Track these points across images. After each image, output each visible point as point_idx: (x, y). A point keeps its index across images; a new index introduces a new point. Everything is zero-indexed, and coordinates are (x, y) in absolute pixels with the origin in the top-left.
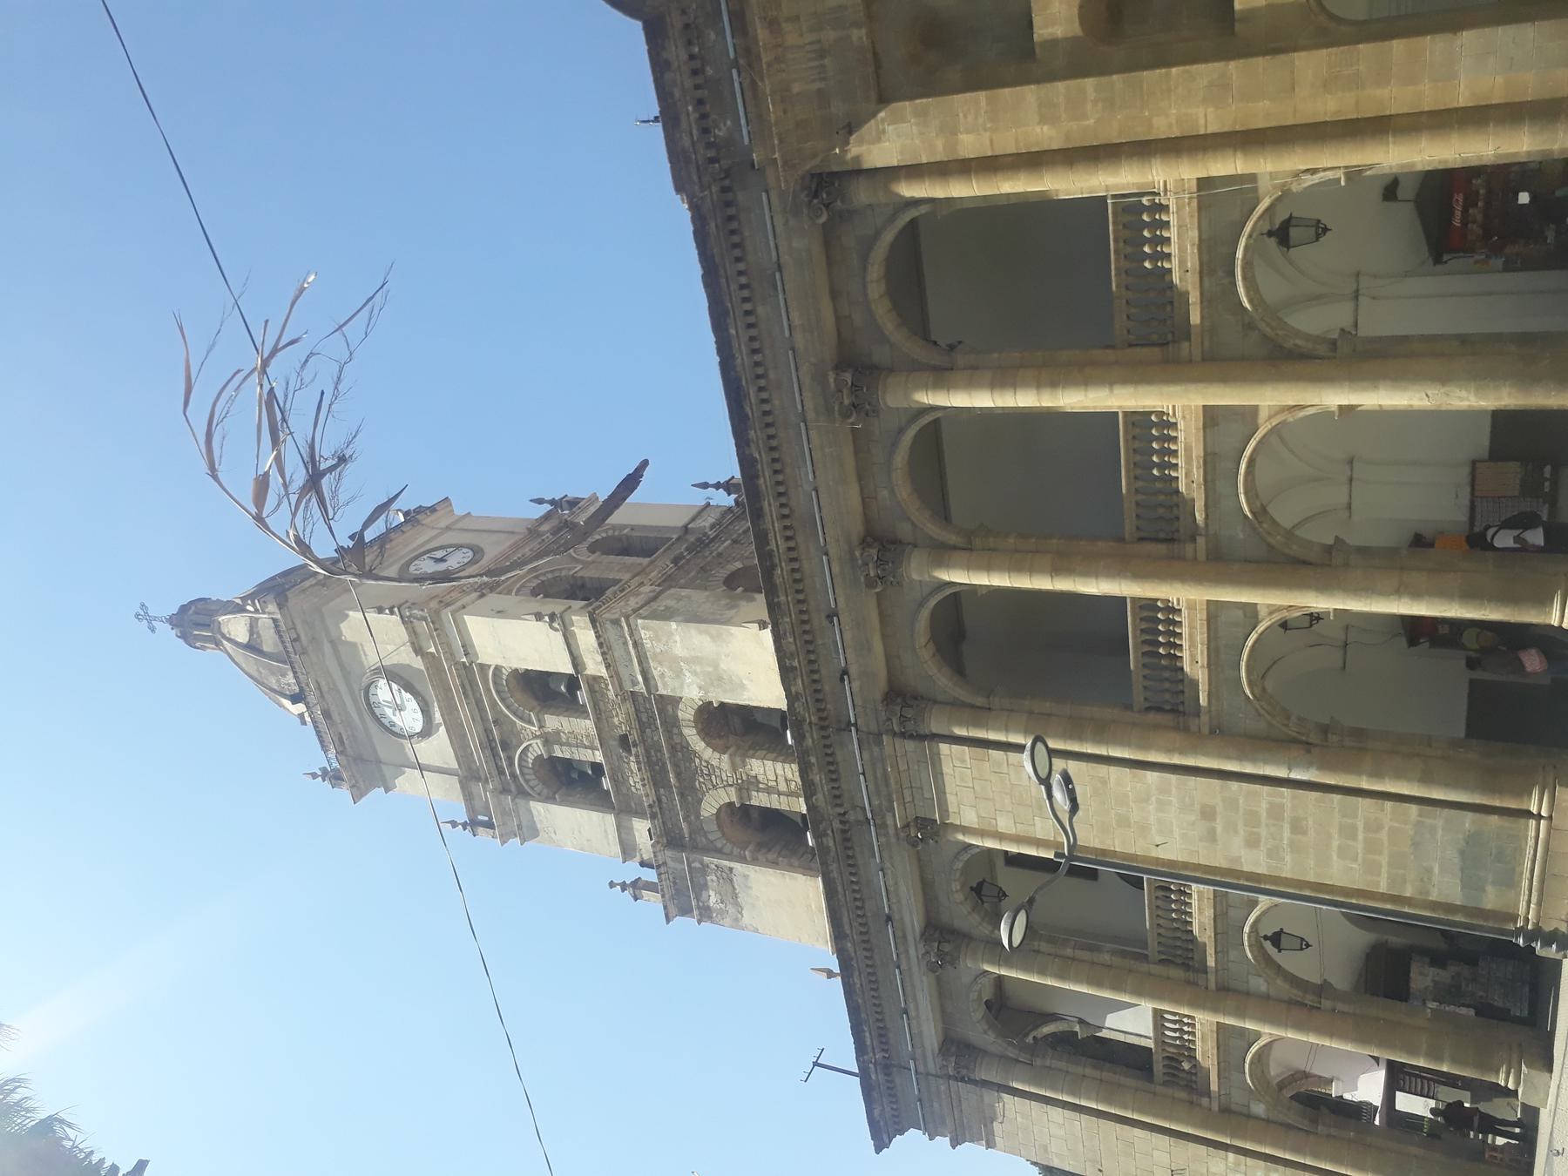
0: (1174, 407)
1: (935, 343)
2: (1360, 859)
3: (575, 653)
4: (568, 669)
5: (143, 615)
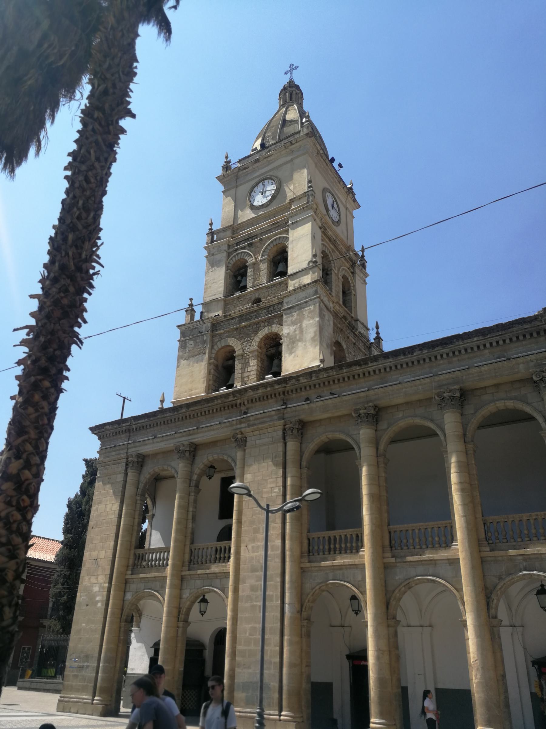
0: (457, 545)
3: (298, 275)
4: (290, 271)
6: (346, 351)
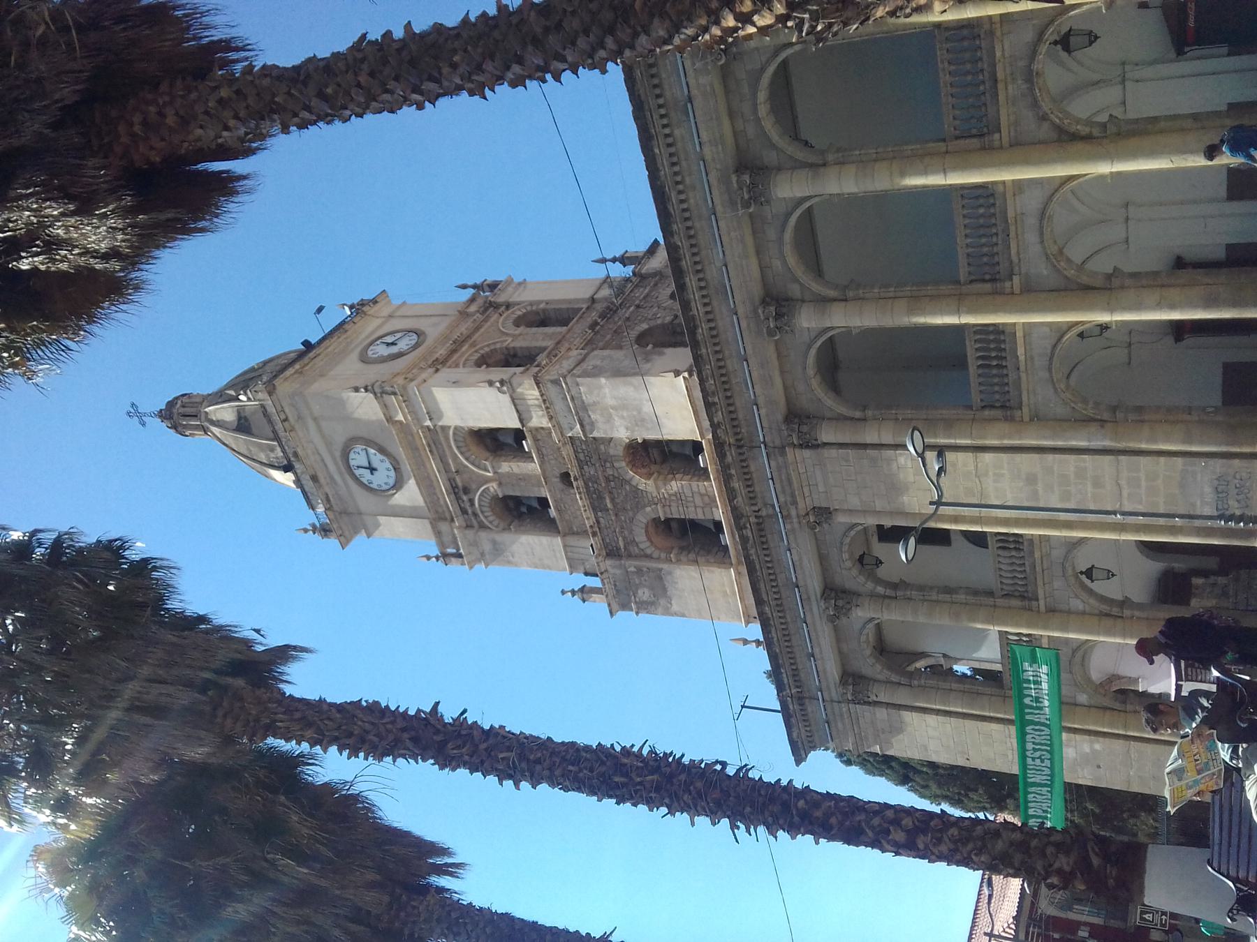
1: (806, 143)
4: (516, 424)
5: (135, 412)
6: (653, 323)
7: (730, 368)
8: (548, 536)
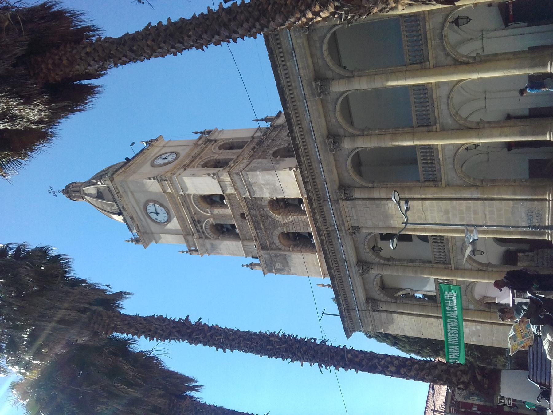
2: (496, 220)
4: (220, 193)
5: (51, 191)
6: (280, 147)
7: (314, 166)
8: (235, 241)
